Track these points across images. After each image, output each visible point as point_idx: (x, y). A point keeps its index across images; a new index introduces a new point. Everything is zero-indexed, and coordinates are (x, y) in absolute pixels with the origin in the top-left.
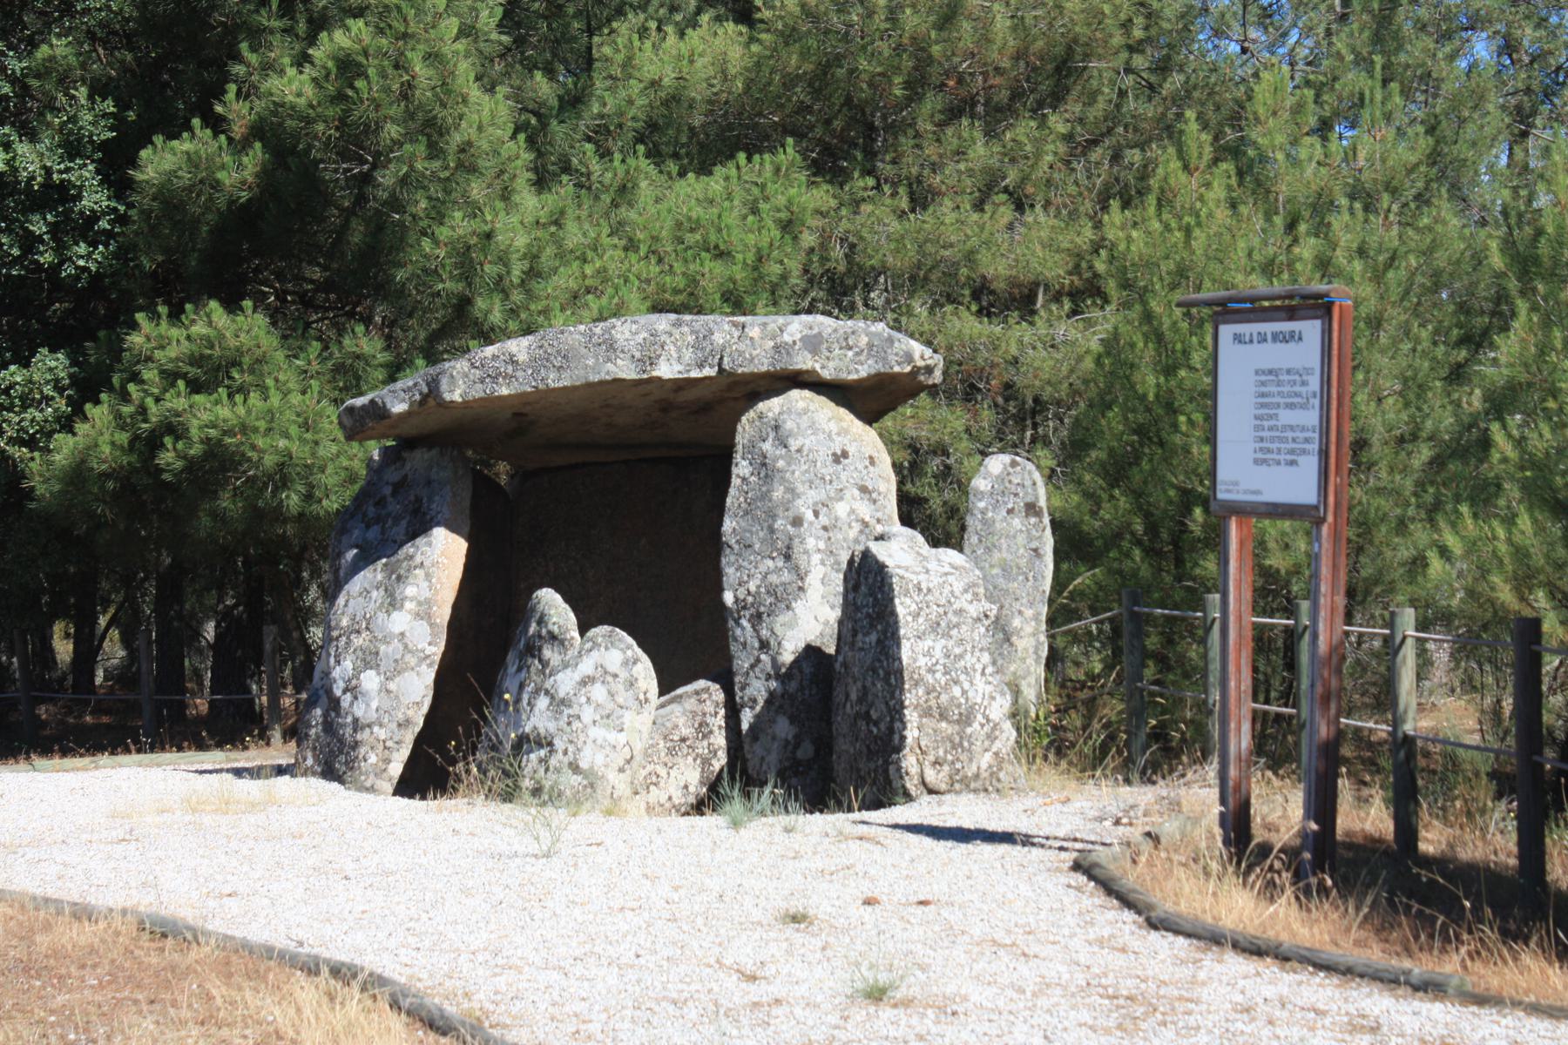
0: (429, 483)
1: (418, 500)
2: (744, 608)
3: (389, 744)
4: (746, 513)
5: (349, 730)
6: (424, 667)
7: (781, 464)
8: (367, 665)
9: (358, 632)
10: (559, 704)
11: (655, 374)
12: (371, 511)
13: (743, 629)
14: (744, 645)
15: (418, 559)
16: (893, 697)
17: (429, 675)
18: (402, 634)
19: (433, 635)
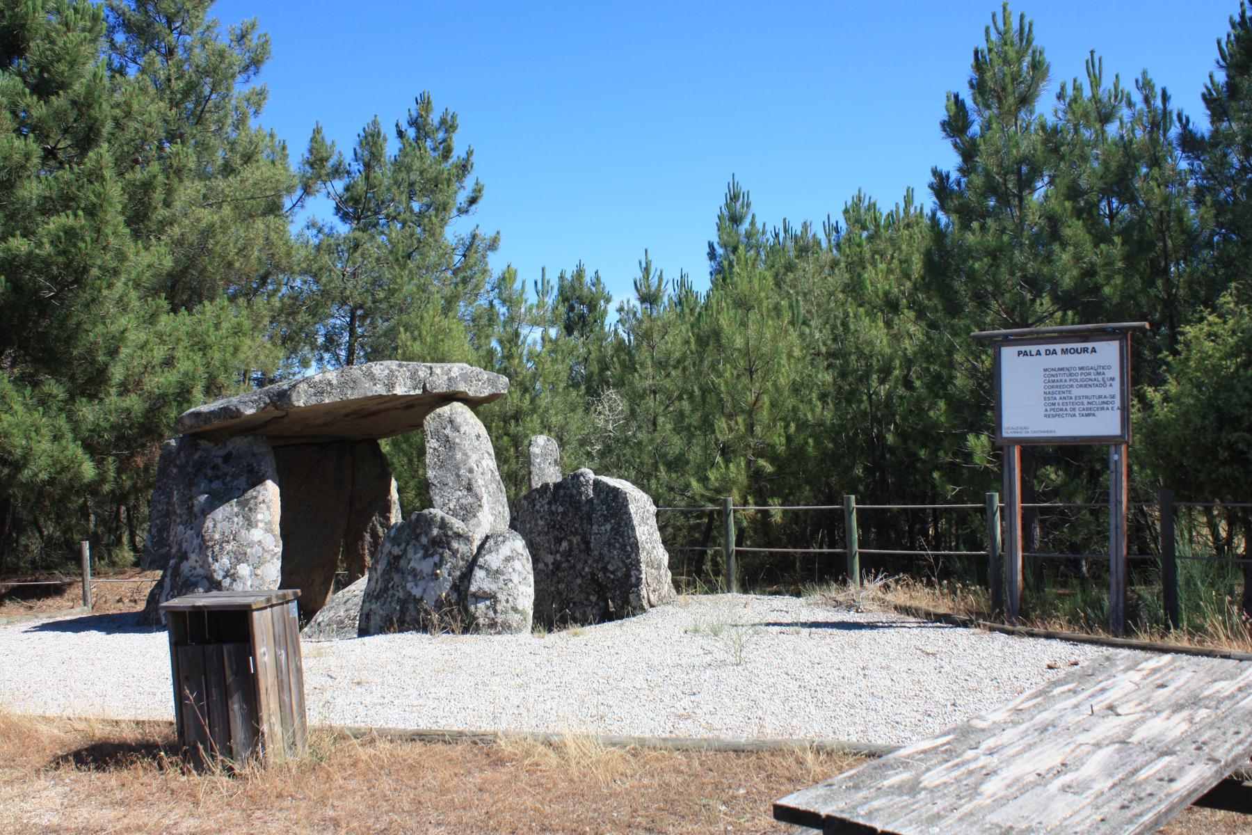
0: (254, 455)
4: (441, 467)
7: (457, 440)
8: (239, 561)
10: (495, 574)
12: (210, 473)
15: (261, 498)
16: (629, 557)
17: (278, 564)
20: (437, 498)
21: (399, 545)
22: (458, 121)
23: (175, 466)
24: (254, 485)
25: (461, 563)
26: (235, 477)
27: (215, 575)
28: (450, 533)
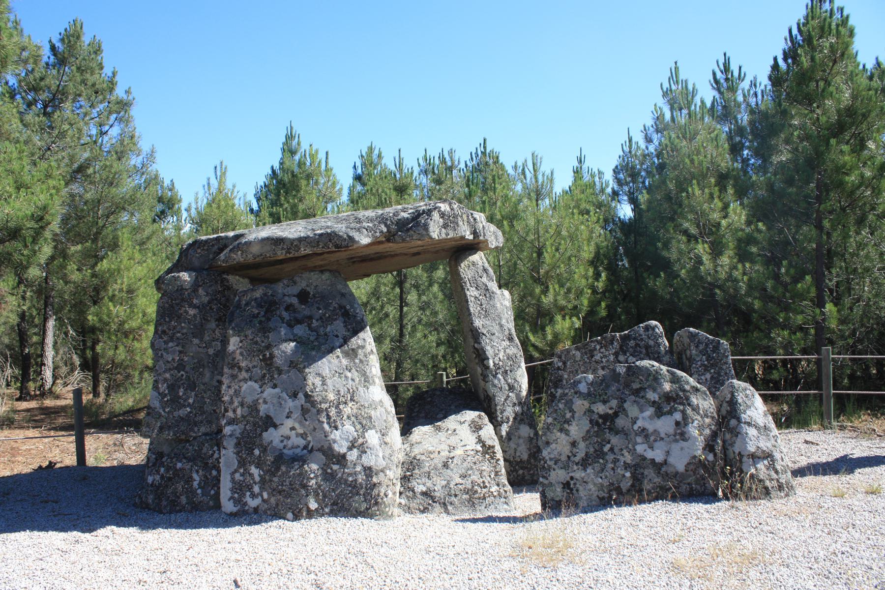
1: (341, 307)
2: (499, 368)
5: (361, 478)
9: (346, 403)
13: (499, 380)
14: (501, 389)
18: (381, 401)
20: (488, 348)
21: (605, 402)
22: (103, 47)
23: (192, 305)
25: (707, 420)
26: (325, 321)
27: (336, 447)
28: (687, 387)
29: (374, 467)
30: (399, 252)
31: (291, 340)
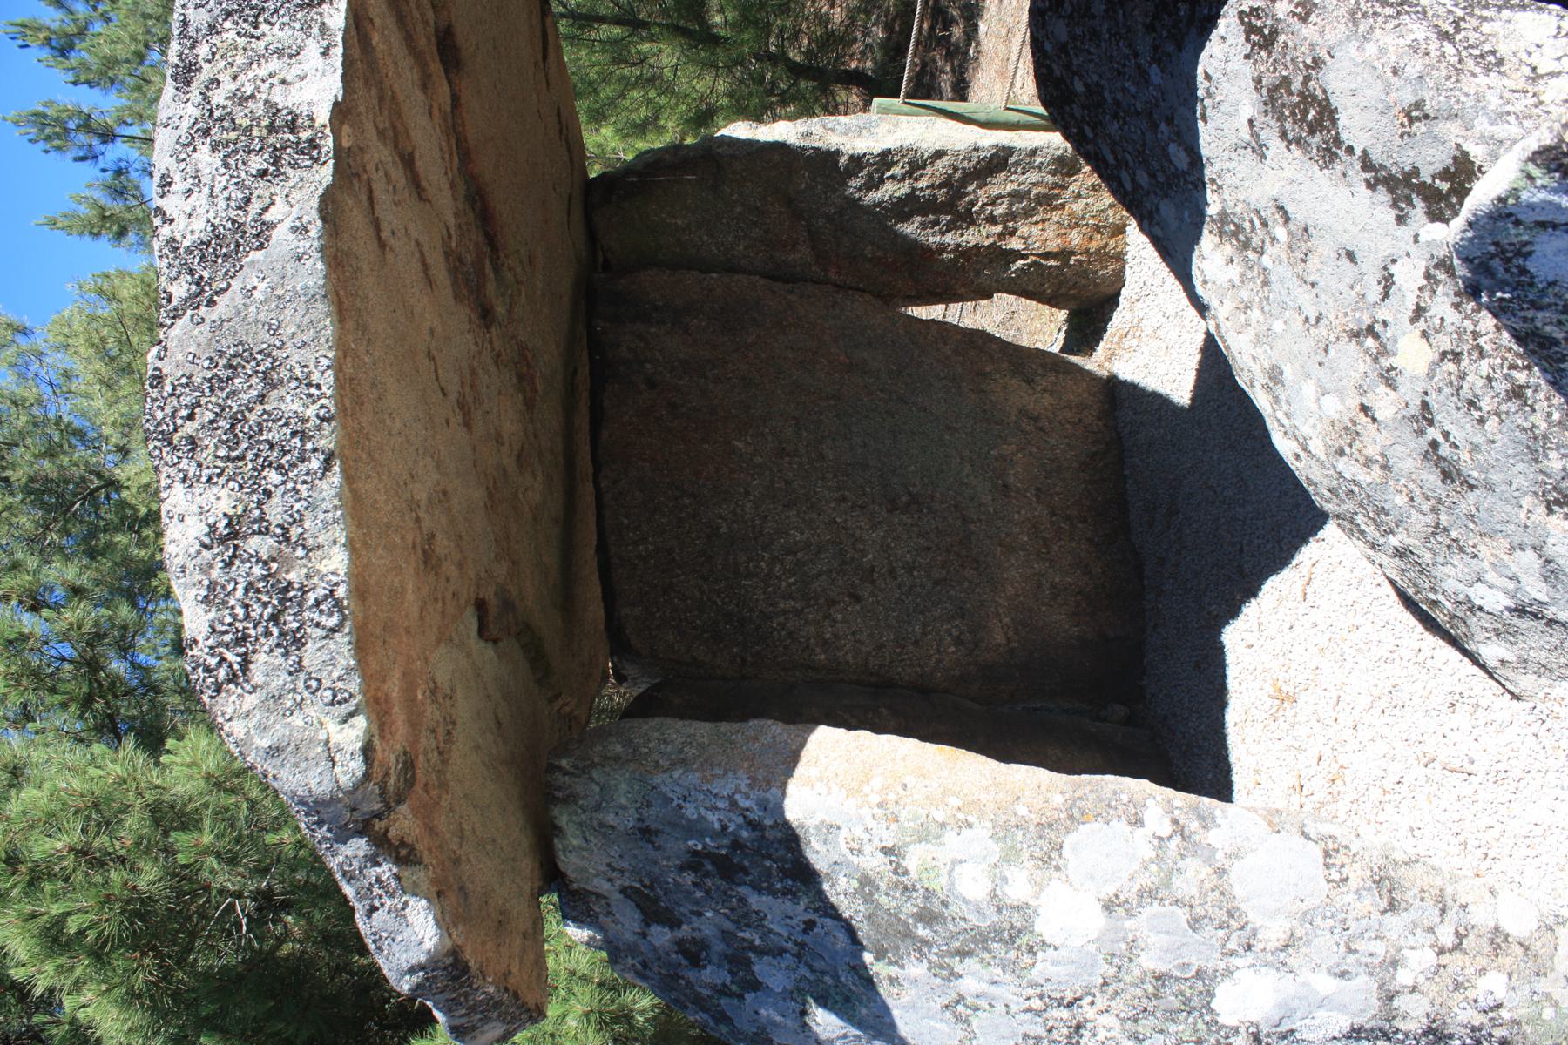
0: (646, 833)
1: (694, 862)
3: (1448, 940)
6: (1213, 837)
11: (323, 116)
12: (712, 975)
15: (873, 862)
18: (1109, 906)
19: (1107, 810)
24: (804, 877)
29: (1359, 1021)
30: (445, 201)
31: (804, 1013)
